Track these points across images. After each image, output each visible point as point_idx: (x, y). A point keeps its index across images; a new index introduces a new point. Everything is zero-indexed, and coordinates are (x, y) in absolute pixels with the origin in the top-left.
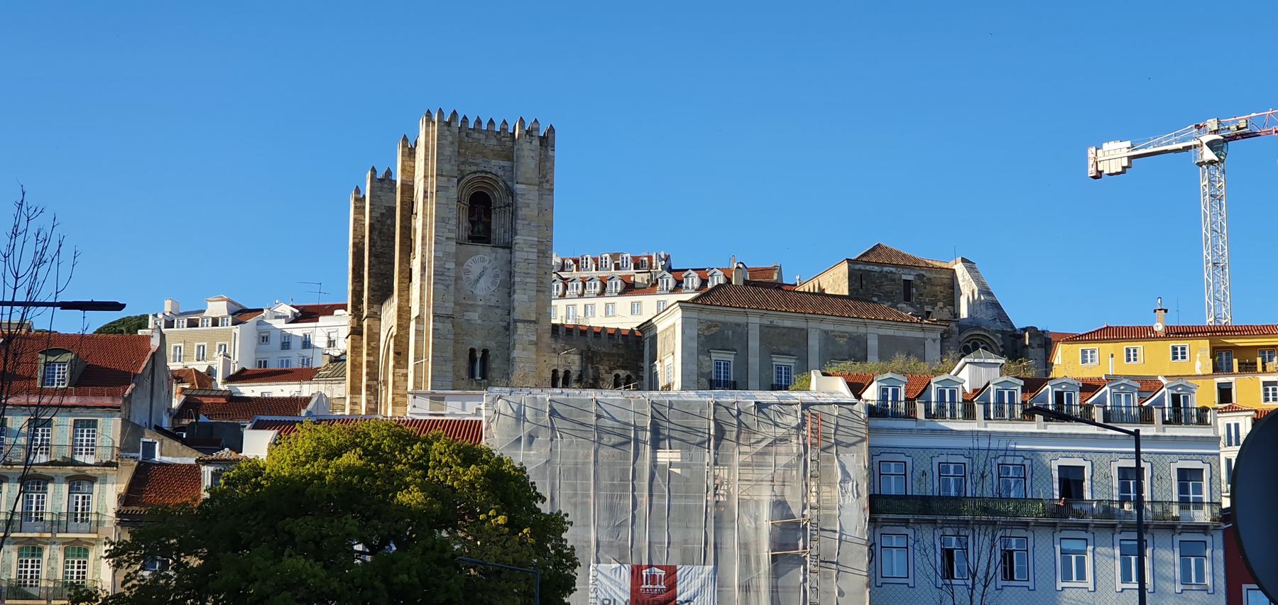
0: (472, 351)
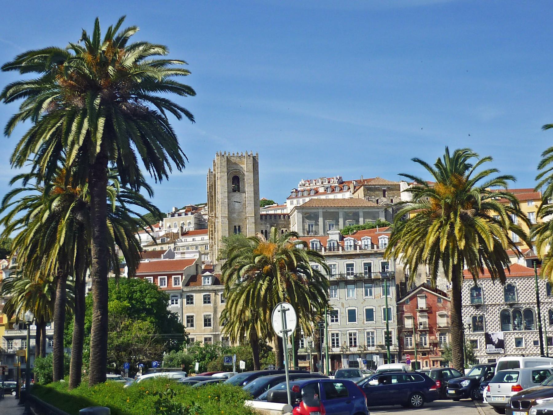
0: (235, 226)
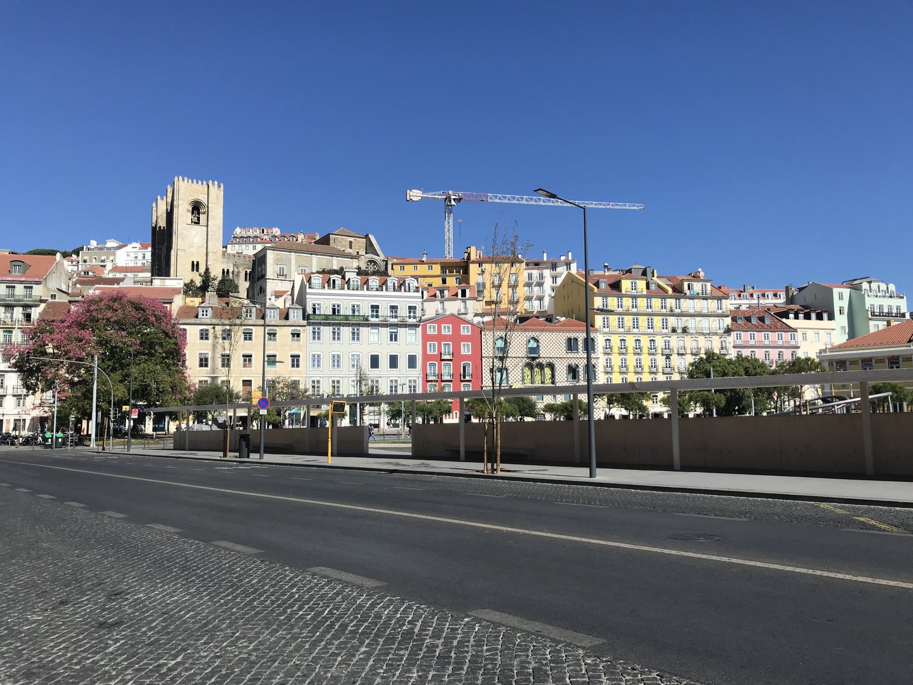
0: (193, 262)
